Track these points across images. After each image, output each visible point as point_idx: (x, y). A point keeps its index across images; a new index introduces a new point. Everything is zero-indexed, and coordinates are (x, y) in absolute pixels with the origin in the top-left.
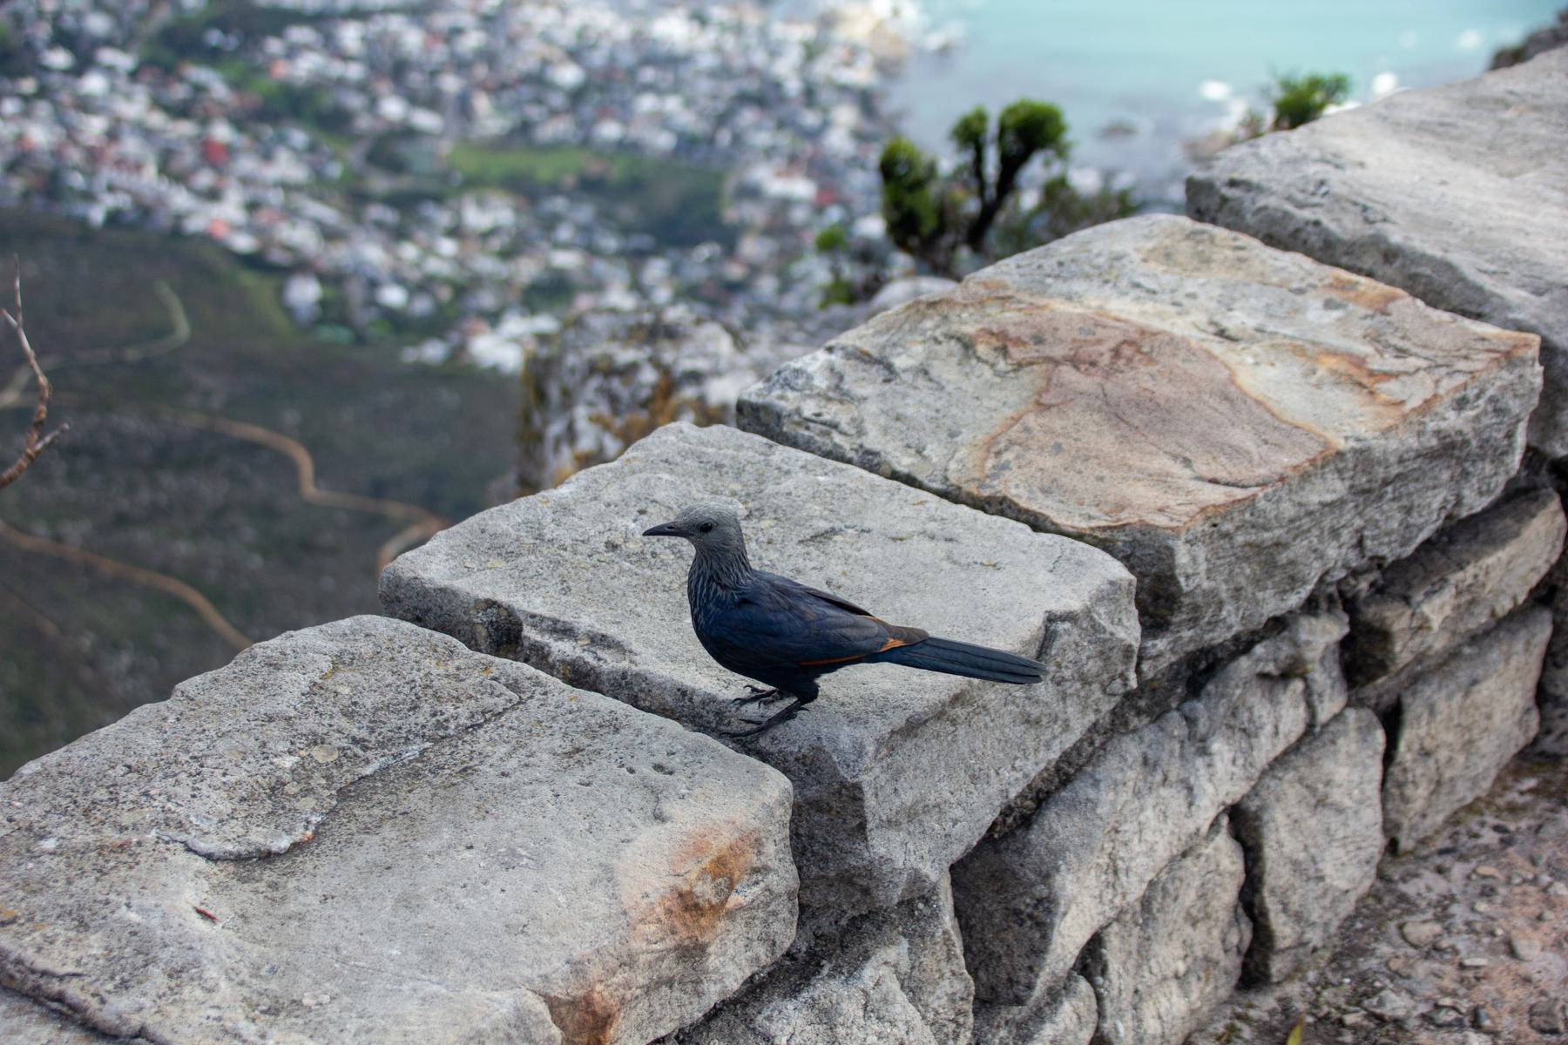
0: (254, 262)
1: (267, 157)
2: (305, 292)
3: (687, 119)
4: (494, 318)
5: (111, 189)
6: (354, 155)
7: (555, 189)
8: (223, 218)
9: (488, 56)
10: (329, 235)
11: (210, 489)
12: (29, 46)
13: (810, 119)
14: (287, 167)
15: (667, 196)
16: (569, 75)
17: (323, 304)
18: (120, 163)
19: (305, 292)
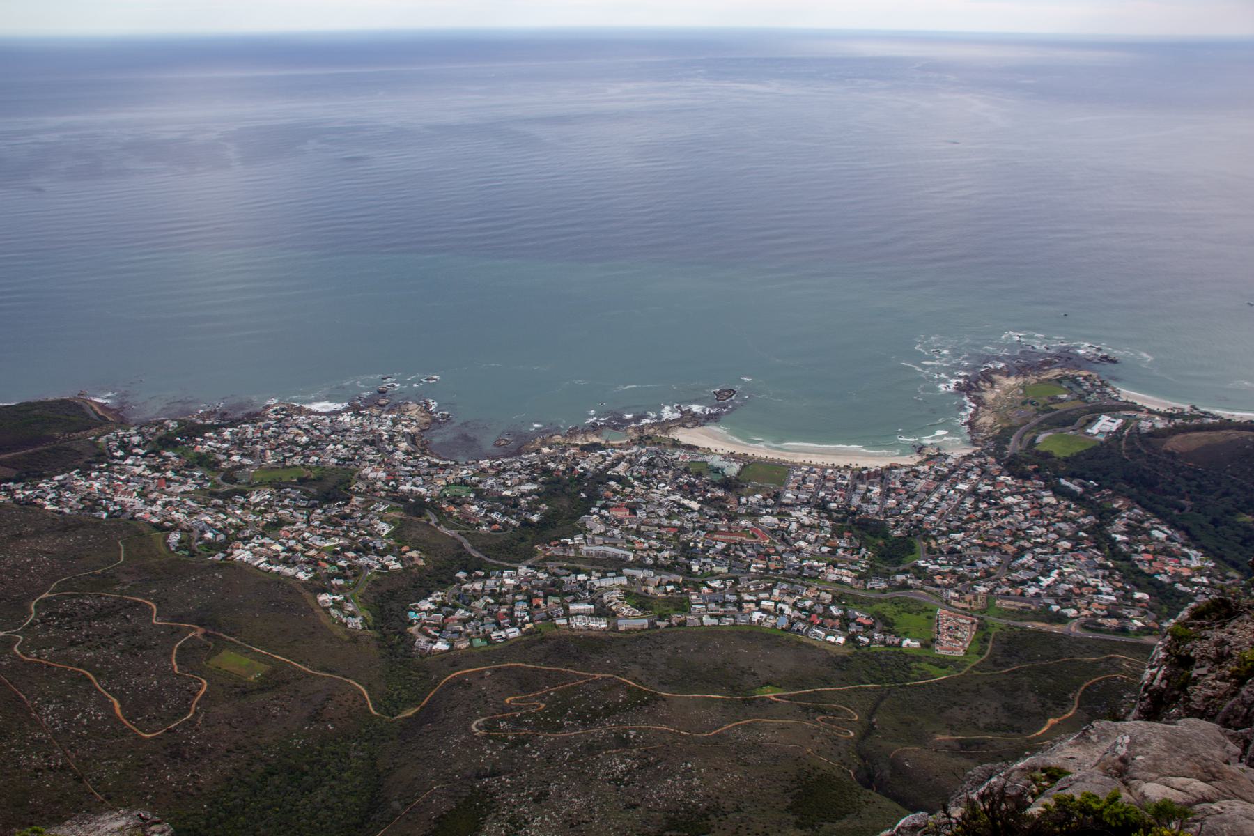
0: (159, 527)
1: (182, 484)
2: (174, 538)
3: (343, 452)
4: (246, 540)
5: (116, 504)
6: (218, 478)
7: (289, 484)
8: (150, 513)
9: (276, 436)
10: (190, 514)
11: (112, 625)
12: (110, 450)
13: (390, 448)
14: (190, 486)
15: (330, 483)
16: (305, 439)
17: (180, 541)
18: (123, 493)
19: (174, 538)
